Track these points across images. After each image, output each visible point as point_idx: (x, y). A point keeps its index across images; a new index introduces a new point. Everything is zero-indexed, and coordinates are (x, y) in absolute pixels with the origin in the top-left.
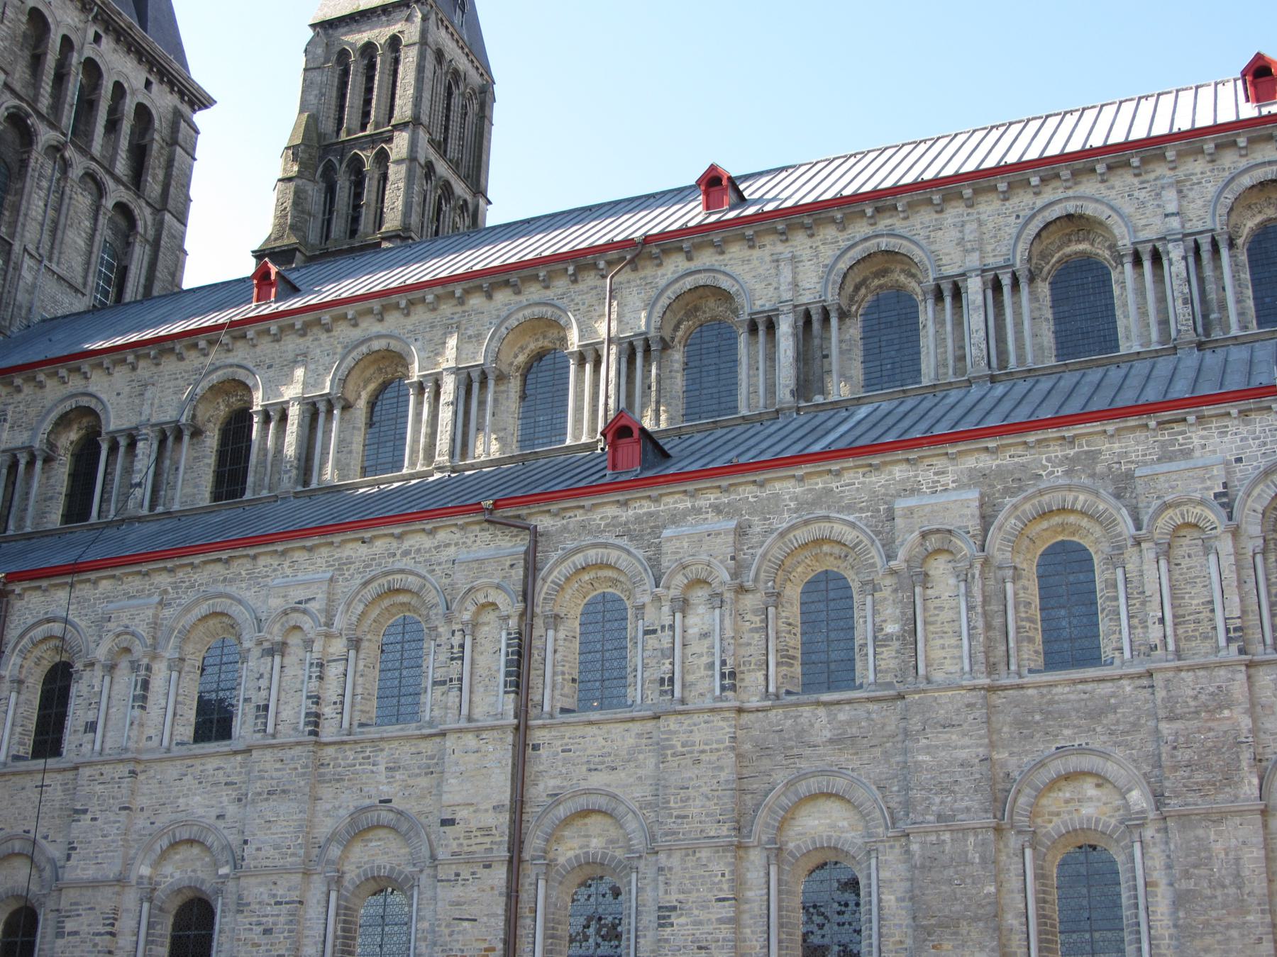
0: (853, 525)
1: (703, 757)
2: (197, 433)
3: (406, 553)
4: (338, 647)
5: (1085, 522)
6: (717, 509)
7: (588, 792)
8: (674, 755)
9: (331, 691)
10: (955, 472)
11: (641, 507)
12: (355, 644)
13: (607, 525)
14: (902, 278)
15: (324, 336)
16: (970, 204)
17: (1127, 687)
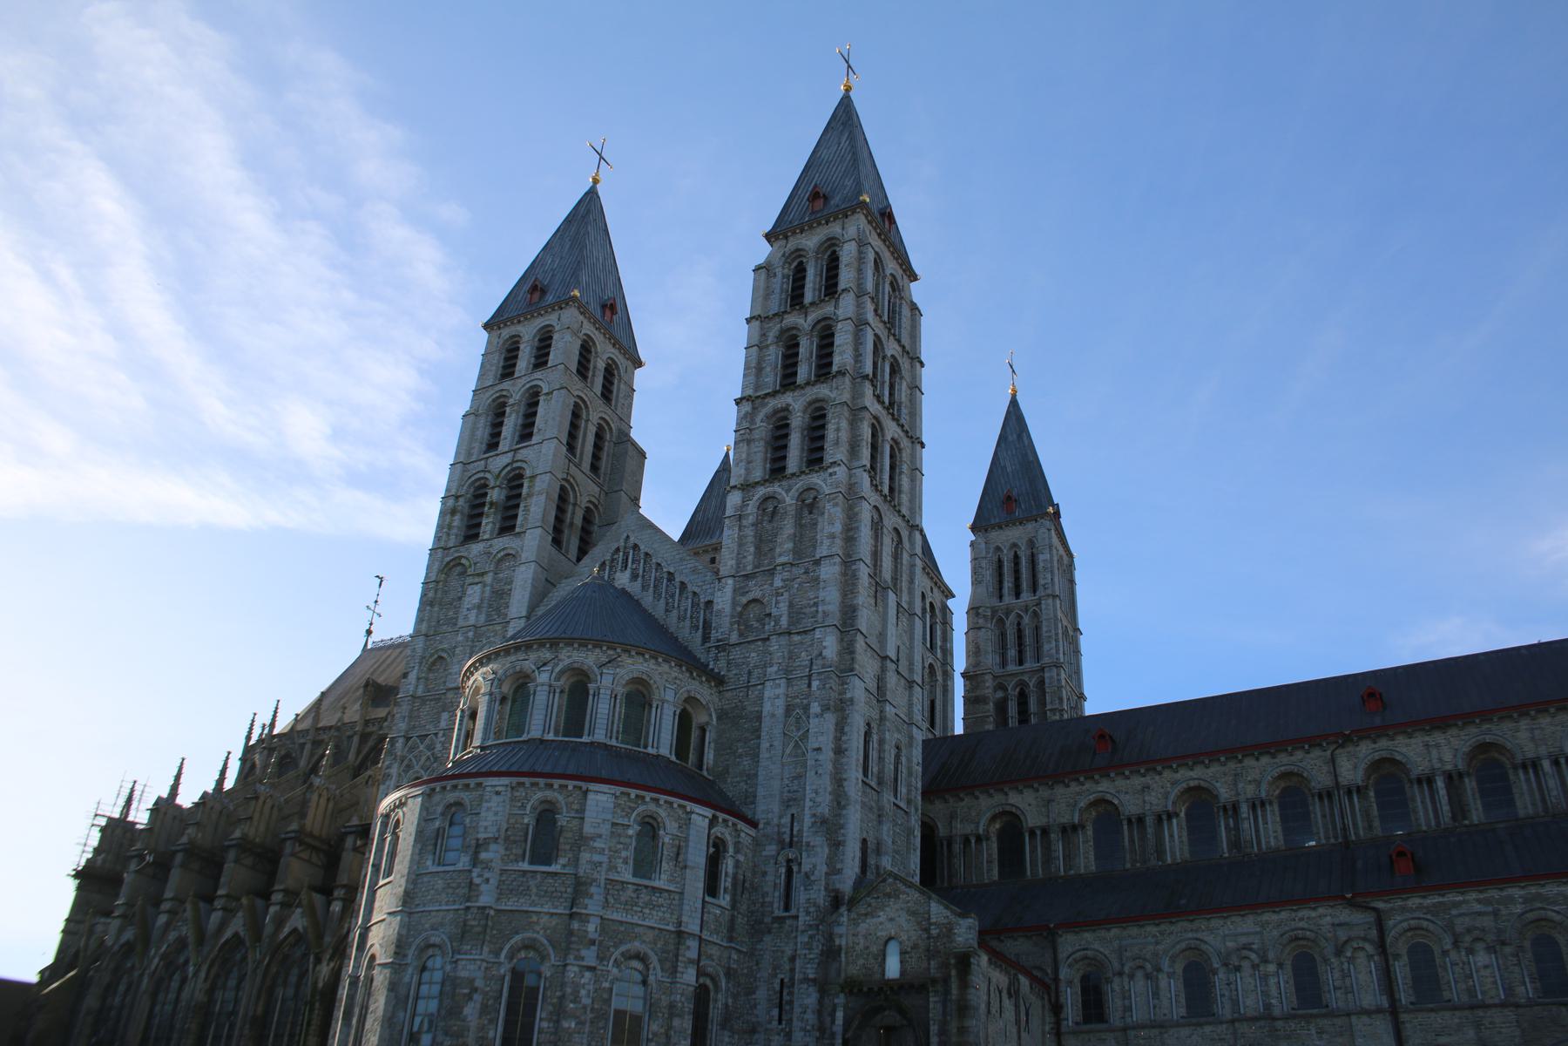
0: (1558, 912)
1: (1503, 1030)
2: (1083, 827)
3: (1301, 919)
4: (1272, 968)
8: (1486, 1028)
9: (1274, 991)
12: (1280, 965)
14: (1496, 755)
15: (1157, 777)
16: (1533, 719)
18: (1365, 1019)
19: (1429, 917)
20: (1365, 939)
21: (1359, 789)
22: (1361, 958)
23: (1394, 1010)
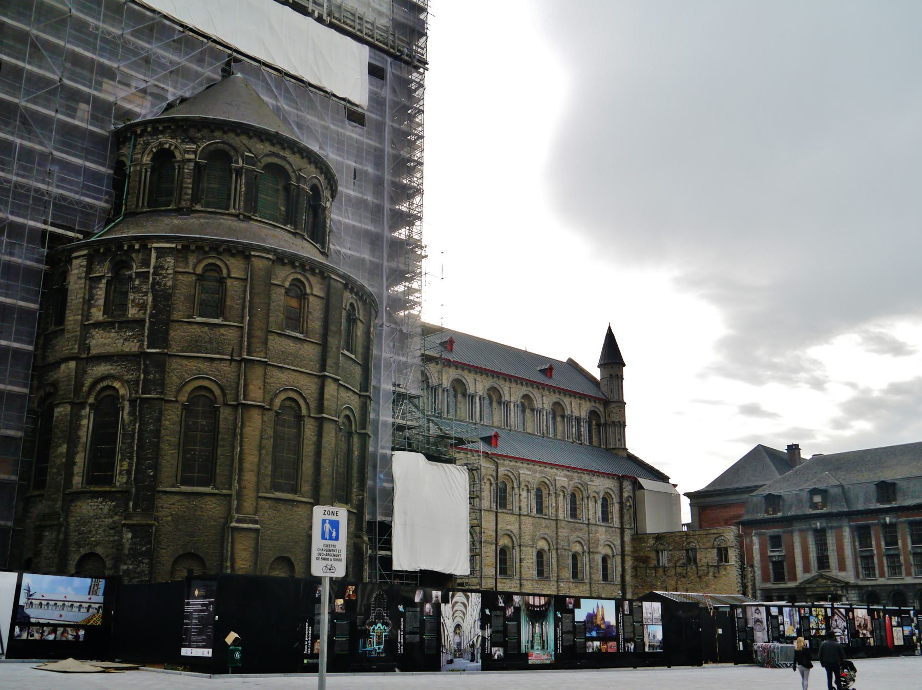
7: (507, 530)
14: (492, 393)
17: (585, 526)
18: (487, 513)
20: (492, 476)
22: (488, 485)
23: (496, 513)
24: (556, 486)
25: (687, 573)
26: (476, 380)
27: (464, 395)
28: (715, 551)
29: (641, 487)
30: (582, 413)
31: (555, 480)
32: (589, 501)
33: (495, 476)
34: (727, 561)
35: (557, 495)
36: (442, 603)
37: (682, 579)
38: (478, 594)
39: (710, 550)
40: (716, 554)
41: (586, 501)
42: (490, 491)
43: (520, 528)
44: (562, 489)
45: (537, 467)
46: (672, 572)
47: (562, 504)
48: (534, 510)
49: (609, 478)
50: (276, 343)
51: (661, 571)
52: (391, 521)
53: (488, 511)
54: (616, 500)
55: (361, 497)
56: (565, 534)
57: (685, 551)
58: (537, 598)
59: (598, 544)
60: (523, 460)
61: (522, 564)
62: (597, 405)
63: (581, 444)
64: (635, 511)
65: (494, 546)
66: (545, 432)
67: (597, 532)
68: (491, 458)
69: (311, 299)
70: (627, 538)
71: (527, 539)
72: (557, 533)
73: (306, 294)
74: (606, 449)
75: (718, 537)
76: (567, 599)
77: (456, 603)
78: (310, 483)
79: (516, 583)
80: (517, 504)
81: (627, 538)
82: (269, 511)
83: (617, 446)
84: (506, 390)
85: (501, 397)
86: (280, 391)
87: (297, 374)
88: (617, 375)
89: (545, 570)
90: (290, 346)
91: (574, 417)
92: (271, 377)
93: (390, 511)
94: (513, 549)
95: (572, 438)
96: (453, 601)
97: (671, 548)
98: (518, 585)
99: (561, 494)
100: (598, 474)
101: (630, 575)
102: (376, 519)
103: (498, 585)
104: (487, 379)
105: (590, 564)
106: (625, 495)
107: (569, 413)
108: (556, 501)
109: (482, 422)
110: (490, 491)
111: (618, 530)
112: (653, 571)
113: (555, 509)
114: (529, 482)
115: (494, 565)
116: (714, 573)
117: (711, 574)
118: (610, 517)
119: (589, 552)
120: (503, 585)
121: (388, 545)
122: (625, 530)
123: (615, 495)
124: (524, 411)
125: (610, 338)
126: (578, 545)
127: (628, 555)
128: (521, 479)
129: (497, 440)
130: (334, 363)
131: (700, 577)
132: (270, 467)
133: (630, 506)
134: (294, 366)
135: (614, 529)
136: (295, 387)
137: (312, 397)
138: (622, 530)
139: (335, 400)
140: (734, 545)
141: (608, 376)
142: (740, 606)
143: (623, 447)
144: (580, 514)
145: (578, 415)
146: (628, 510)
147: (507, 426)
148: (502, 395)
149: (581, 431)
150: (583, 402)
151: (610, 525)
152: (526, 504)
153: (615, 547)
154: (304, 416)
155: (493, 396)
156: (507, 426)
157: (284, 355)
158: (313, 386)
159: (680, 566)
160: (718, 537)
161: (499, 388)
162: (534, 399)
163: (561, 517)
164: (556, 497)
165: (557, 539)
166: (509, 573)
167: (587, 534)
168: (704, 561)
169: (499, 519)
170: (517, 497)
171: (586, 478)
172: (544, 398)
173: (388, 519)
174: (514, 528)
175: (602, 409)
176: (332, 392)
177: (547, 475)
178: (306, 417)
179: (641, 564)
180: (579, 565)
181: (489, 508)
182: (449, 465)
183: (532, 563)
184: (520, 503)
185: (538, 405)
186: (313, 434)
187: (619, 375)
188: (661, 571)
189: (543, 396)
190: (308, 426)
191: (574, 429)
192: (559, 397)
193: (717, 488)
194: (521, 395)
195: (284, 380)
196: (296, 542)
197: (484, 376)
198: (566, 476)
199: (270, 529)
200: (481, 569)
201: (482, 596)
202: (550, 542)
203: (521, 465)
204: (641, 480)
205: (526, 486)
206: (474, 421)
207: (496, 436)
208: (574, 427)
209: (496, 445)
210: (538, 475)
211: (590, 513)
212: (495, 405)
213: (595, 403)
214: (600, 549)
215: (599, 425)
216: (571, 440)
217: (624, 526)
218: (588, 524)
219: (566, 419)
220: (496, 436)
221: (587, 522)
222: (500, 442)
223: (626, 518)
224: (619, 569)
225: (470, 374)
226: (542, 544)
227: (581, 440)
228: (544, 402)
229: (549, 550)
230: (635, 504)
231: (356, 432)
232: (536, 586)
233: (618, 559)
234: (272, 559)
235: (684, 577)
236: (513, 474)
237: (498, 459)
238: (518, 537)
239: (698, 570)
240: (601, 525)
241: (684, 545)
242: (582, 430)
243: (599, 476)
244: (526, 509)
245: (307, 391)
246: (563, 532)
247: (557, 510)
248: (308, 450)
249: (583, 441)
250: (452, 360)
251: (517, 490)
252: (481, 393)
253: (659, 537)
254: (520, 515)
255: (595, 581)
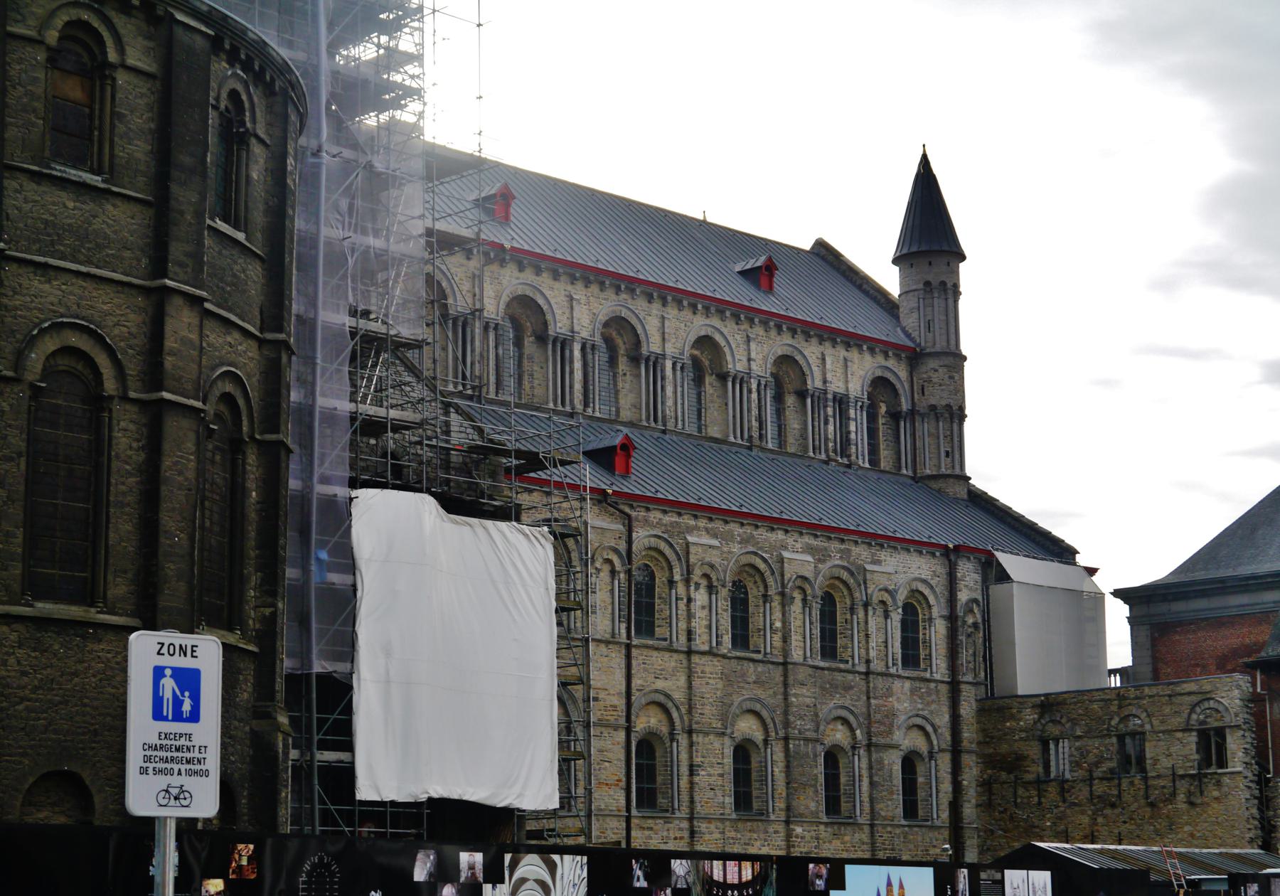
1: (711, 681)
5: (841, 586)
6: (707, 530)
7: (656, 691)
8: (698, 677)
10: (801, 542)
11: (672, 517)
13: (657, 523)
14: (614, 334)
18: (603, 648)
19: (666, 536)
20: (616, 551)
21: (496, 327)
22: (605, 575)
23: (628, 647)
24: (782, 575)
25: (1119, 796)
26: (571, 299)
27: (542, 338)
28: (1193, 738)
29: (1004, 577)
30: (850, 385)
31: (781, 560)
32: (870, 613)
33: (624, 554)
34: (1222, 763)
35: (786, 600)
36: (486, 881)
37: (1108, 811)
38: (579, 858)
39: (1179, 735)
40: (1194, 747)
41: (861, 614)
42: (612, 591)
43: (690, 687)
44: (799, 583)
45: (735, 528)
46: (1082, 793)
47: (799, 623)
48: (727, 639)
49: (921, 553)
50: (26, 201)
51: (1052, 791)
52: (351, 674)
53: (607, 643)
54: (938, 609)
55: (268, 611)
56: (808, 701)
57: (1114, 740)
58: (732, 866)
59: (892, 725)
60: (697, 510)
61: (696, 779)
62: (891, 363)
63: (849, 466)
64: (988, 639)
65: (621, 735)
66: (755, 434)
67: (889, 693)
68: (614, 506)
69: (122, 78)
70: (967, 709)
71: (707, 713)
72: (786, 700)
73: (106, 64)
74: (913, 478)
75: (1200, 702)
76: (811, 866)
77: (523, 881)
78: (130, 575)
79: (681, 829)
80: (682, 625)
81: (967, 709)
82: (20, 653)
83: (943, 470)
84: (652, 325)
85: (638, 343)
86: (43, 332)
87: (87, 284)
88: (943, 284)
89: (755, 793)
90: (68, 207)
91: (830, 396)
92: (15, 293)
93: (347, 647)
94: (672, 740)
95: (827, 451)
96: (517, 875)
97: (1079, 733)
98: (686, 834)
99: (798, 596)
100: (892, 543)
101: (973, 801)
102: (310, 667)
103: (633, 833)
104: (602, 295)
105: (871, 777)
106: (963, 596)
107: (819, 384)
108: (784, 615)
109: (590, 410)
110: (612, 591)
111: (944, 689)
112: (1034, 793)
113: (780, 634)
114: (712, 566)
115: (623, 784)
116: (1190, 793)
117: (1181, 797)
118: (922, 654)
119: (869, 746)
120: (647, 833)
121: (343, 736)
122: (963, 687)
123: (936, 597)
124: (699, 381)
125: (926, 184)
126: (840, 727)
127: (969, 752)
128: (692, 559)
129: (629, 456)
130: (187, 255)
131: (1152, 805)
132: (20, 533)
133: (975, 625)
134: (80, 263)
135: (932, 685)
136: (83, 319)
137: (131, 347)
138: (954, 687)
139: (195, 353)
140: (1240, 720)
141: (921, 286)
142: (1254, 878)
143: (957, 471)
144: (845, 647)
145: (842, 391)
146: (969, 636)
147: (656, 420)
148: (642, 337)
149: (849, 432)
150: (854, 355)
151: (923, 674)
152: (705, 623)
153: (935, 731)
154: (111, 398)
155: (619, 341)
156: (656, 420)
157: (50, 230)
158: (132, 316)
159: (1102, 779)
160: (1200, 702)
161: (634, 321)
162: (726, 350)
163: (796, 655)
164: (783, 605)
165: (786, 713)
166: (661, 801)
167: (865, 698)
168: (1166, 763)
169: (634, 662)
170: (682, 605)
171: (861, 553)
172: (753, 345)
173: (341, 667)
174: (675, 686)
175: (903, 374)
176: (185, 333)
177: (761, 548)
178: (116, 401)
179: (1004, 775)
180: (843, 779)
181: (608, 636)
182: (503, 525)
183: (722, 775)
184: (689, 622)
185: (735, 363)
186: (135, 445)
187: (949, 285)
188: (1052, 791)
189: (748, 340)
190: (123, 424)
191: (831, 428)
192: (790, 341)
193: (1200, 575)
194: (692, 338)
195: (51, 299)
196: (96, 733)
197: (594, 288)
198: (809, 550)
199: (22, 699)
200: (589, 792)
201: (588, 863)
202: (769, 721)
203: (692, 522)
204: (1005, 559)
205: (706, 576)
206: (568, 409)
207: (627, 447)
208: (831, 420)
209: (627, 472)
210: (736, 549)
211: (872, 644)
212: (623, 365)
213: (886, 356)
214: (898, 736)
215: (895, 416)
216: (823, 457)
217: (960, 678)
218: (867, 674)
219: (809, 401)
220: (627, 447)
221: (862, 669)
222: (636, 462)
223: (965, 656)
224: (947, 787)
225: (557, 285)
226: (747, 727)
227: (849, 456)
228: (753, 355)
229: (766, 741)
230: (987, 620)
231: (252, 437)
232: (733, 834)
233: (945, 762)
234: (31, 780)
235: (1113, 806)
236: (671, 546)
237: (631, 507)
238: (683, 710)
239: (1147, 787)
240: (899, 677)
241: (1113, 723)
242: (852, 427)
243: (895, 548)
244: (705, 637)
245: (116, 332)
246: (802, 696)
247: (786, 639)
248: (123, 488)
249: (853, 458)
250: (507, 246)
251: (681, 589)
252: (585, 334)
253: (1048, 705)
254: (689, 653)
255: (885, 818)
